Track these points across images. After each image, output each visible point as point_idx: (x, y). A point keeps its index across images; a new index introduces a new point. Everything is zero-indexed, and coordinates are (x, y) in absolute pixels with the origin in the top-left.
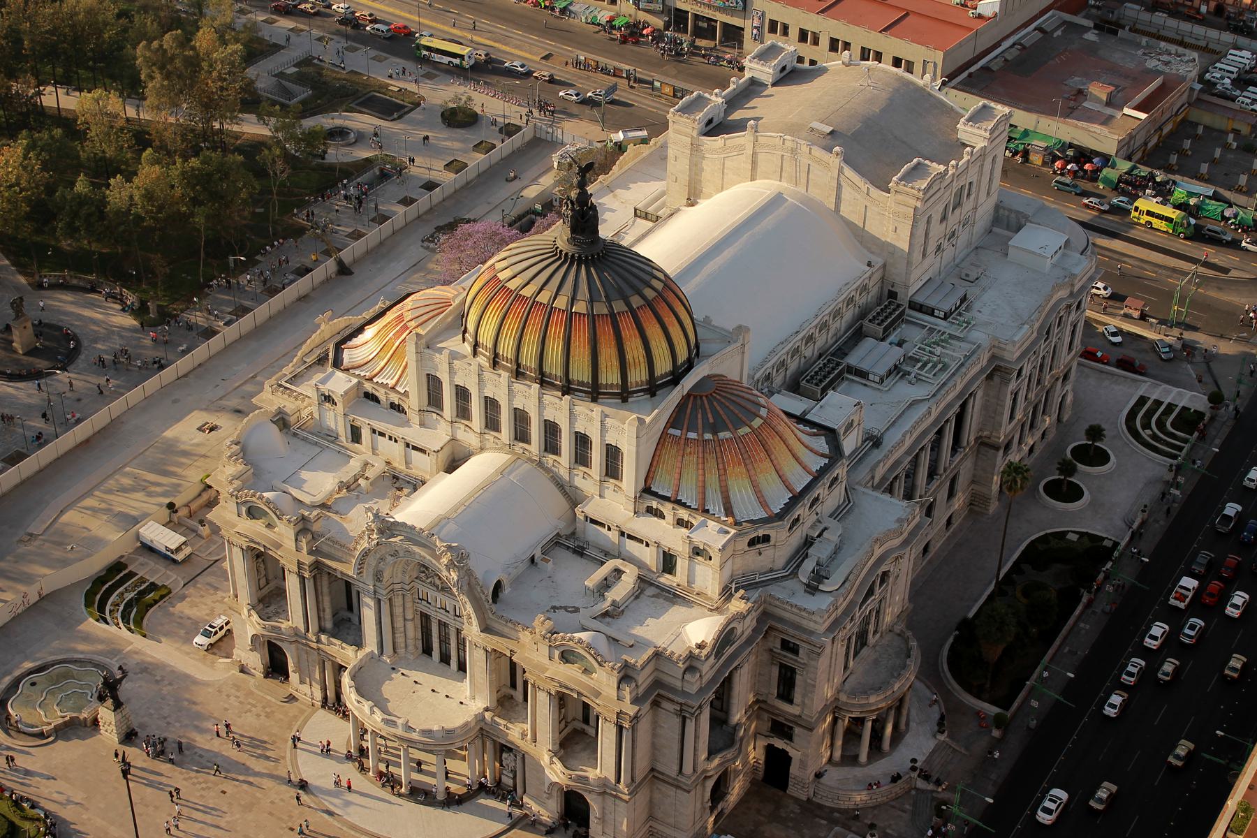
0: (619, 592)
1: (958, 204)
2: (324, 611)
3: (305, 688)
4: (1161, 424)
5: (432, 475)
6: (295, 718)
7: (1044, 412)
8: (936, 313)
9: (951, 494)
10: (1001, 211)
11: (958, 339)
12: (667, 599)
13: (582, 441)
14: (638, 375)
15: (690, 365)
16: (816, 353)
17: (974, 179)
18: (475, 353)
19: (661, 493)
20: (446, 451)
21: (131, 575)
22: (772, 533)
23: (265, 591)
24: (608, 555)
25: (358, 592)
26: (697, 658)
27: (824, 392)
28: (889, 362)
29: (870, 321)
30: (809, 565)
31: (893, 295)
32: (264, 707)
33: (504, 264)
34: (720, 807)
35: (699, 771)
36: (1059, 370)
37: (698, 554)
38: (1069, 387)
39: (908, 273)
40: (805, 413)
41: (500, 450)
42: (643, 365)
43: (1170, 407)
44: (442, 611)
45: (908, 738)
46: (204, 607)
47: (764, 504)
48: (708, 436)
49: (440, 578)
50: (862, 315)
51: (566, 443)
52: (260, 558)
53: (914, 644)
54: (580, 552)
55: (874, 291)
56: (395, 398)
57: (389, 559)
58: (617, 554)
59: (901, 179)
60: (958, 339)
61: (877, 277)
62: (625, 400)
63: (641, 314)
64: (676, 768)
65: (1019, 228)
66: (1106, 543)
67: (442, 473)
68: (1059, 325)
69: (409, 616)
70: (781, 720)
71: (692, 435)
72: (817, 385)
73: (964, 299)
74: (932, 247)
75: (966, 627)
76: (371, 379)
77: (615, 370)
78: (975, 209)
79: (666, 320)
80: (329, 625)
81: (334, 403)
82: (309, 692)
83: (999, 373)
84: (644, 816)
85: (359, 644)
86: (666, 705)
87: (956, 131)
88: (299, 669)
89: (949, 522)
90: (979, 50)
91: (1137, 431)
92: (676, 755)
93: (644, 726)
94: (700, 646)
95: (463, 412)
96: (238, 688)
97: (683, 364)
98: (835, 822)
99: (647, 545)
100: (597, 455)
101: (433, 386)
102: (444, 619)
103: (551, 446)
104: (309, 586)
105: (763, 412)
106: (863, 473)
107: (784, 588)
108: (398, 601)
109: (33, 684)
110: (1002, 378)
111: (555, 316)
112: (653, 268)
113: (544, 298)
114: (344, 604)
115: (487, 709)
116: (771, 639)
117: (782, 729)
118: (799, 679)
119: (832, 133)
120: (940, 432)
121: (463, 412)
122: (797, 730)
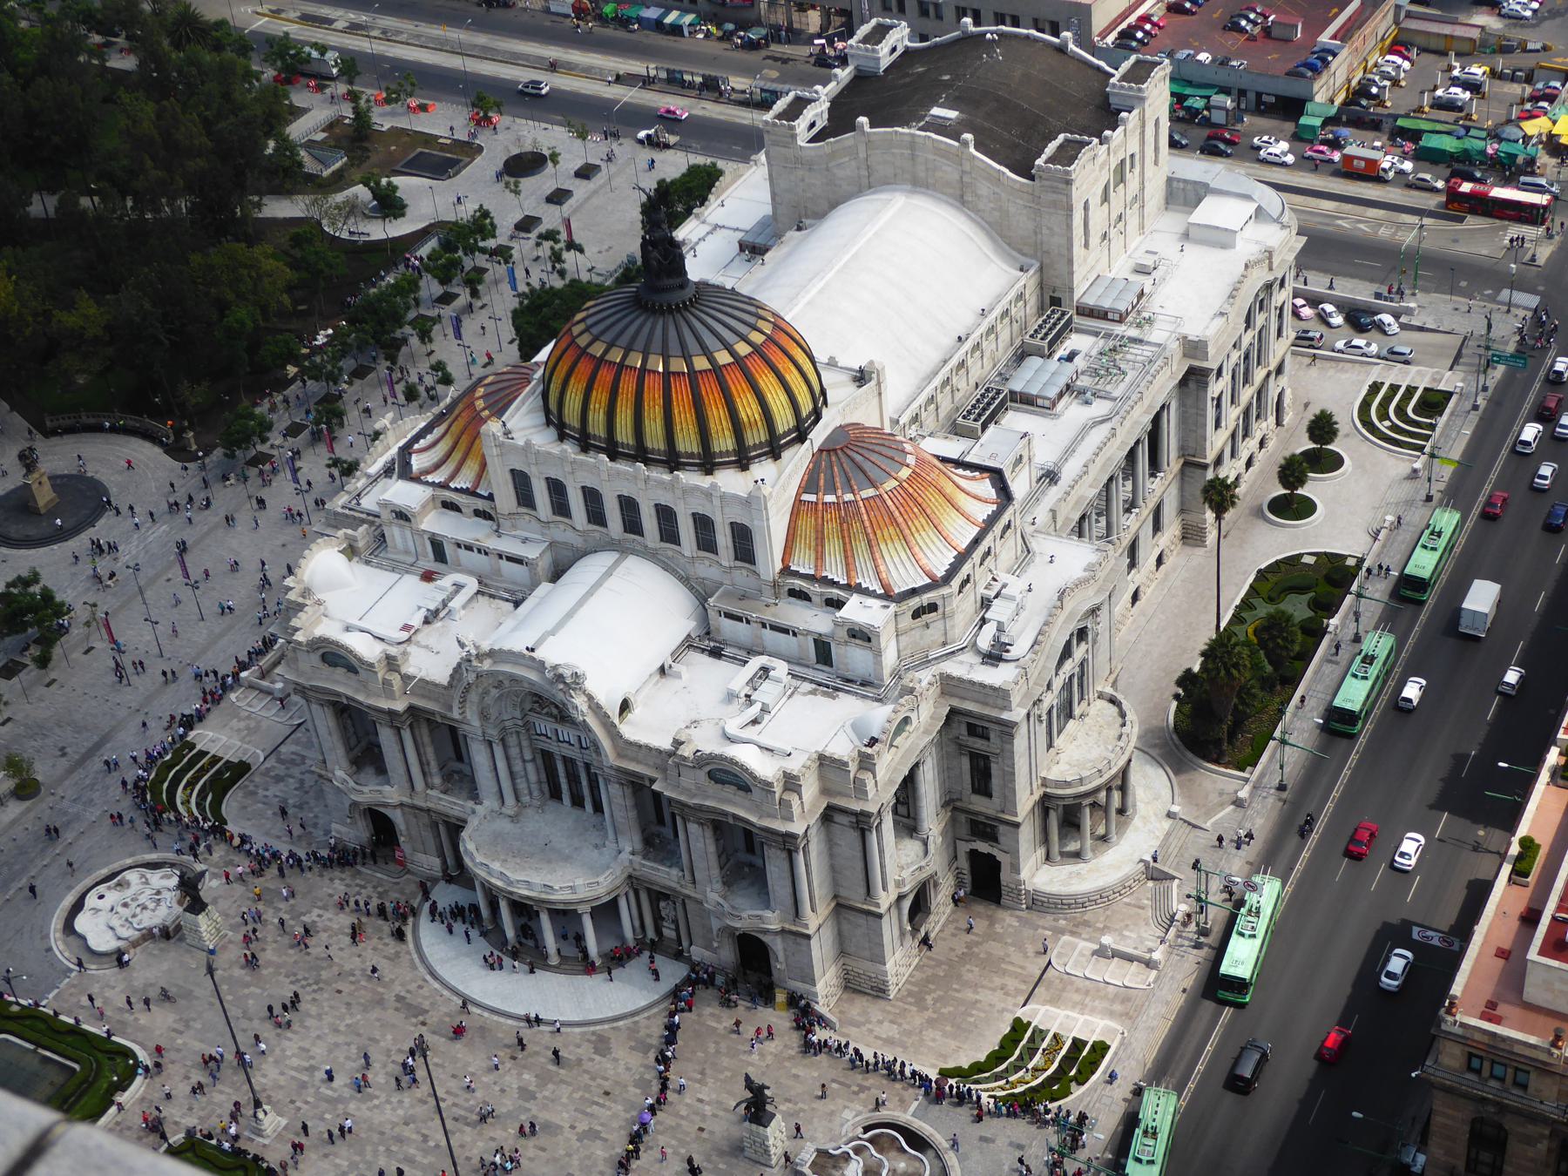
0: (767, 692)
2: (428, 764)
4: (1400, 410)
7: (1258, 417)
8: (1110, 316)
9: (1157, 527)
10: (1175, 184)
11: (1141, 341)
12: (825, 694)
13: (703, 524)
16: (972, 382)
18: (562, 437)
19: (802, 571)
21: (203, 754)
22: (939, 603)
23: (357, 751)
24: (752, 652)
25: (465, 737)
26: (870, 757)
27: (984, 427)
28: (1062, 382)
29: (1032, 336)
30: (989, 630)
31: (1056, 302)
32: (375, 887)
33: (582, 327)
35: (891, 886)
37: (854, 636)
38: (1283, 381)
42: (759, 424)
43: (1410, 391)
44: (565, 745)
45: (1137, 821)
46: (291, 780)
48: (849, 497)
49: (557, 707)
54: (716, 653)
56: (481, 504)
57: (494, 692)
58: (761, 650)
59: (1046, 162)
60: (1141, 341)
64: (862, 891)
65: (1200, 201)
66: (1351, 562)
67: (545, 587)
68: (1261, 309)
69: (528, 756)
70: (982, 819)
71: (830, 498)
72: (975, 420)
73: (1141, 295)
75: (1187, 679)
76: (444, 486)
77: (727, 433)
78: (1142, 183)
80: (437, 780)
81: (407, 519)
82: (429, 863)
83: (1193, 377)
85: (474, 796)
87: (1107, 96)
89: (1159, 561)
91: (1373, 424)
92: (861, 876)
93: (816, 847)
95: (561, 507)
97: (808, 417)
98: (1062, 932)
99: (795, 634)
100: (724, 539)
101: (521, 482)
103: (669, 533)
104: (407, 735)
105: (910, 460)
106: (1041, 513)
107: (961, 663)
108: (512, 740)
109: (101, 897)
110: (1198, 382)
111: (649, 381)
112: (758, 307)
114: (452, 754)
115: (633, 853)
116: (954, 725)
118: (995, 769)
120: (1131, 455)
121: (561, 507)
122: (1002, 828)
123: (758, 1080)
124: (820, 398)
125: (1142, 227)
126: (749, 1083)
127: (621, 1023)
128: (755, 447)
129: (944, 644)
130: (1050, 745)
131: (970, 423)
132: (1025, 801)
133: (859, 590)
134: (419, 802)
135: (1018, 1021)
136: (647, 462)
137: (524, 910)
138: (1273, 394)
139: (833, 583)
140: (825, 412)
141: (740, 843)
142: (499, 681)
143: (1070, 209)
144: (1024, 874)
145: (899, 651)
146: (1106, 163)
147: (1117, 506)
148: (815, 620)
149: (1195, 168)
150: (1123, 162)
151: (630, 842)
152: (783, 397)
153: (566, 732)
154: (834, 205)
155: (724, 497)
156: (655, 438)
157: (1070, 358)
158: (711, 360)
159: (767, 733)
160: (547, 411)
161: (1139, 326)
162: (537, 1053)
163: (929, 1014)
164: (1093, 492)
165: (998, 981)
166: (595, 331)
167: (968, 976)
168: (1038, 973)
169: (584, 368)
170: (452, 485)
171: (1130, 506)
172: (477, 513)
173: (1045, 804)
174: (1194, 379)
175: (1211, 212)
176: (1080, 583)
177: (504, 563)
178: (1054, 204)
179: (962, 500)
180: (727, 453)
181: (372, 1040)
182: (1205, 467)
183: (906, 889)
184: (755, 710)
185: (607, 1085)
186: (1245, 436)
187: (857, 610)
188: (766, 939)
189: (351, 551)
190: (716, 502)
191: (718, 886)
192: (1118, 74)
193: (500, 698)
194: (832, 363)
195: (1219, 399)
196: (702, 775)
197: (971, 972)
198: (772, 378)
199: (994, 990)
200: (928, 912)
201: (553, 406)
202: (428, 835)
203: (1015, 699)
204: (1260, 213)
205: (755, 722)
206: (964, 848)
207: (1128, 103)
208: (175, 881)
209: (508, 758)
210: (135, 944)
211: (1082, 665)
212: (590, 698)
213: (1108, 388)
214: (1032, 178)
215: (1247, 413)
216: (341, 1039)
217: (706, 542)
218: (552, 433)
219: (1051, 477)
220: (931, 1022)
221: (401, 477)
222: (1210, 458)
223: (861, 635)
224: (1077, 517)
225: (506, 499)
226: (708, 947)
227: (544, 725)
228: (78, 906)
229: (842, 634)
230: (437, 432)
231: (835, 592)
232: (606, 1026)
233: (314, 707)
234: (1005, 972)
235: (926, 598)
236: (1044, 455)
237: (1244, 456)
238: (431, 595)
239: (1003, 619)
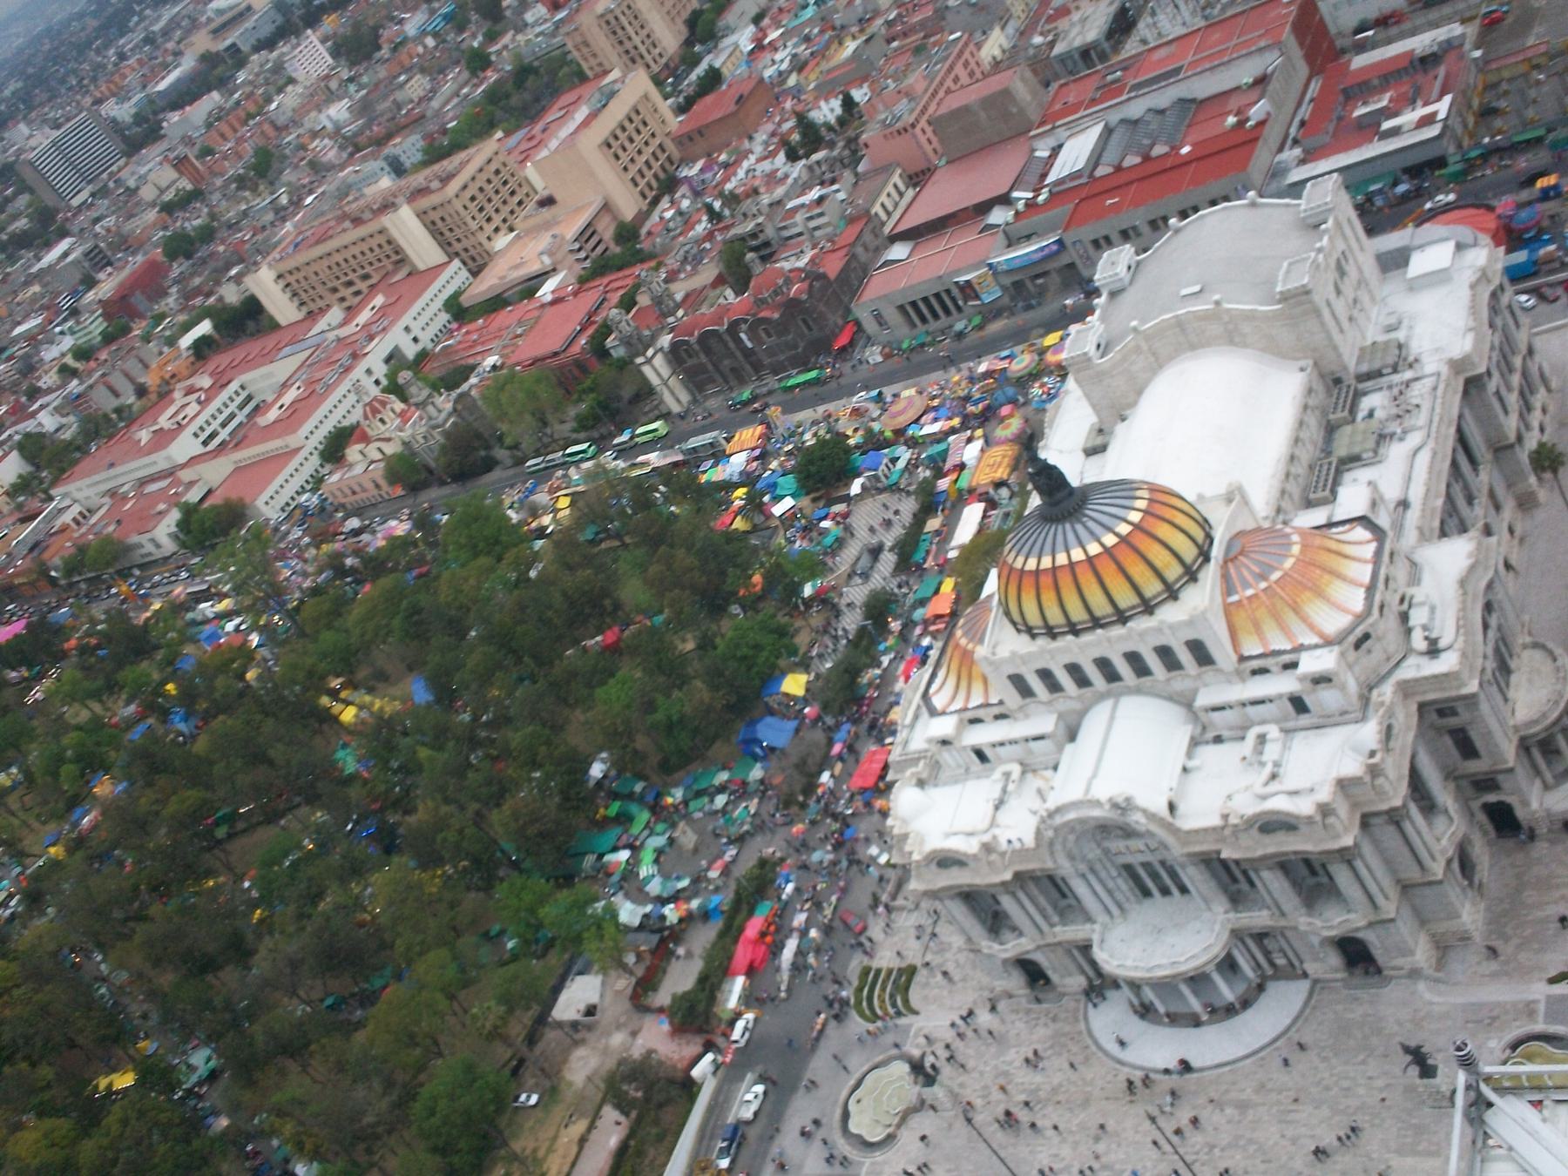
0: (1271, 751)
5: (1060, 749)
6: (1076, 1010)
9: (1498, 507)
11: (1416, 379)
13: (1165, 653)
14: (1173, 571)
15: (1210, 538)
18: (1033, 636)
21: (878, 972)
22: (1370, 630)
23: (989, 922)
25: (1063, 879)
27: (1334, 493)
31: (1338, 381)
34: (1476, 881)
35: (1438, 856)
36: (1523, 348)
38: (1537, 358)
39: (1339, 356)
40: (1329, 517)
41: (1102, 697)
47: (1346, 611)
48: (1263, 585)
50: (1324, 413)
51: (1153, 662)
52: (969, 897)
54: (1218, 740)
55: (1319, 388)
56: (996, 711)
60: (1416, 379)
61: (1315, 374)
63: (1145, 525)
64: (1416, 868)
67: (1069, 747)
69: (1114, 873)
76: (965, 709)
79: (1167, 516)
80: (1056, 919)
85: (1089, 919)
86: (1375, 821)
88: (1055, 970)
93: (1367, 849)
95: (1054, 686)
100: (1184, 656)
101: (1018, 682)
102: (1148, 858)
103: (1141, 669)
106: (1410, 536)
108: (1098, 867)
114: (1056, 895)
117: (1487, 783)
118: (1474, 735)
119: (1201, 291)
120: (1454, 464)
121: (1054, 686)
122: (1500, 778)
123: (1413, 1044)
124: (1205, 524)
125: (1373, 299)
126: (1407, 1050)
127: (1279, 1043)
128: (1177, 580)
129: (1388, 659)
130: (1506, 700)
131: (1320, 494)
132: (1509, 751)
133: (1300, 648)
134: (1050, 940)
136: (1102, 626)
137: (1165, 986)
138: (1534, 371)
140: (1213, 533)
141: (1304, 871)
142: (1070, 827)
143: (1317, 313)
144: (1535, 805)
145: (1357, 679)
146: (1327, 266)
147: (1461, 502)
148: (1280, 685)
149: (1391, 241)
150: (1338, 261)
151: (1220, 906)
152: (1181, 537)
153: (1137, 844)
154: (1140, 392)
155: (1172, 627)
156: (1101, 606)
157: (1371, 415)
158: (1117, 535)
159: (1290, 781)
160: (1014, 623)
161: (1411, 366)
162: (1227, 1091)
163: (1515, 941)
164: (1440, 502)
165: (1557, 894)
166: (1026, 549)
169: (1028, 583)
170: (971, 705)
171: (1470, 500)
172: (998, 717)
173: (1524, 746)
174: (1473, 386)
175: (1420, 264)
176: (1472, 568)
177: (1033, 745)
179: (1349, 550)
180: (1159, 594)
182: (1511, 446)
183: (1450, 853)
184: (1268, 769)
185: (1292, 1094)
187: (1312, 663)
188: (1360, 935)
189: (921, 783)
190: (1167, 631)
191: (1303, 910)
193: (1078, 839)
194: (1201, 497)
195: (1498, 393)
196: (1254, 832)
197: (1530, 896)
198: (1166, 526)
199: (1556, 902)
200: (1473, 867)
202: (1067, 962)
203: (1465, 675)
204: (1460, 247)
205: (1274, 776)
206: (1476, 805)
207: (1321, 217)
208: (906, 1068)
209: (1101, 881)
210: (899, 1126)
212: (1144, 811)
213: (1413, 422)
215: (1522, 393)
218: (1025, 638)
219: (1404, 504)
220: (1519, 947)
222: (1512, 437)
223: (1321, 680)
224: (1437, 524)
225: (1013, 699)
226: (1316, 959)
227: (1117, 845)
228: (846, 1115)
229: (1308, 685)
230: (941, 674)
231: (1287, 658)
234: (1558, 886)
235: (1359, 632)
236: (1392, 493)
237: (1535, 424)
239: (1424, 621)
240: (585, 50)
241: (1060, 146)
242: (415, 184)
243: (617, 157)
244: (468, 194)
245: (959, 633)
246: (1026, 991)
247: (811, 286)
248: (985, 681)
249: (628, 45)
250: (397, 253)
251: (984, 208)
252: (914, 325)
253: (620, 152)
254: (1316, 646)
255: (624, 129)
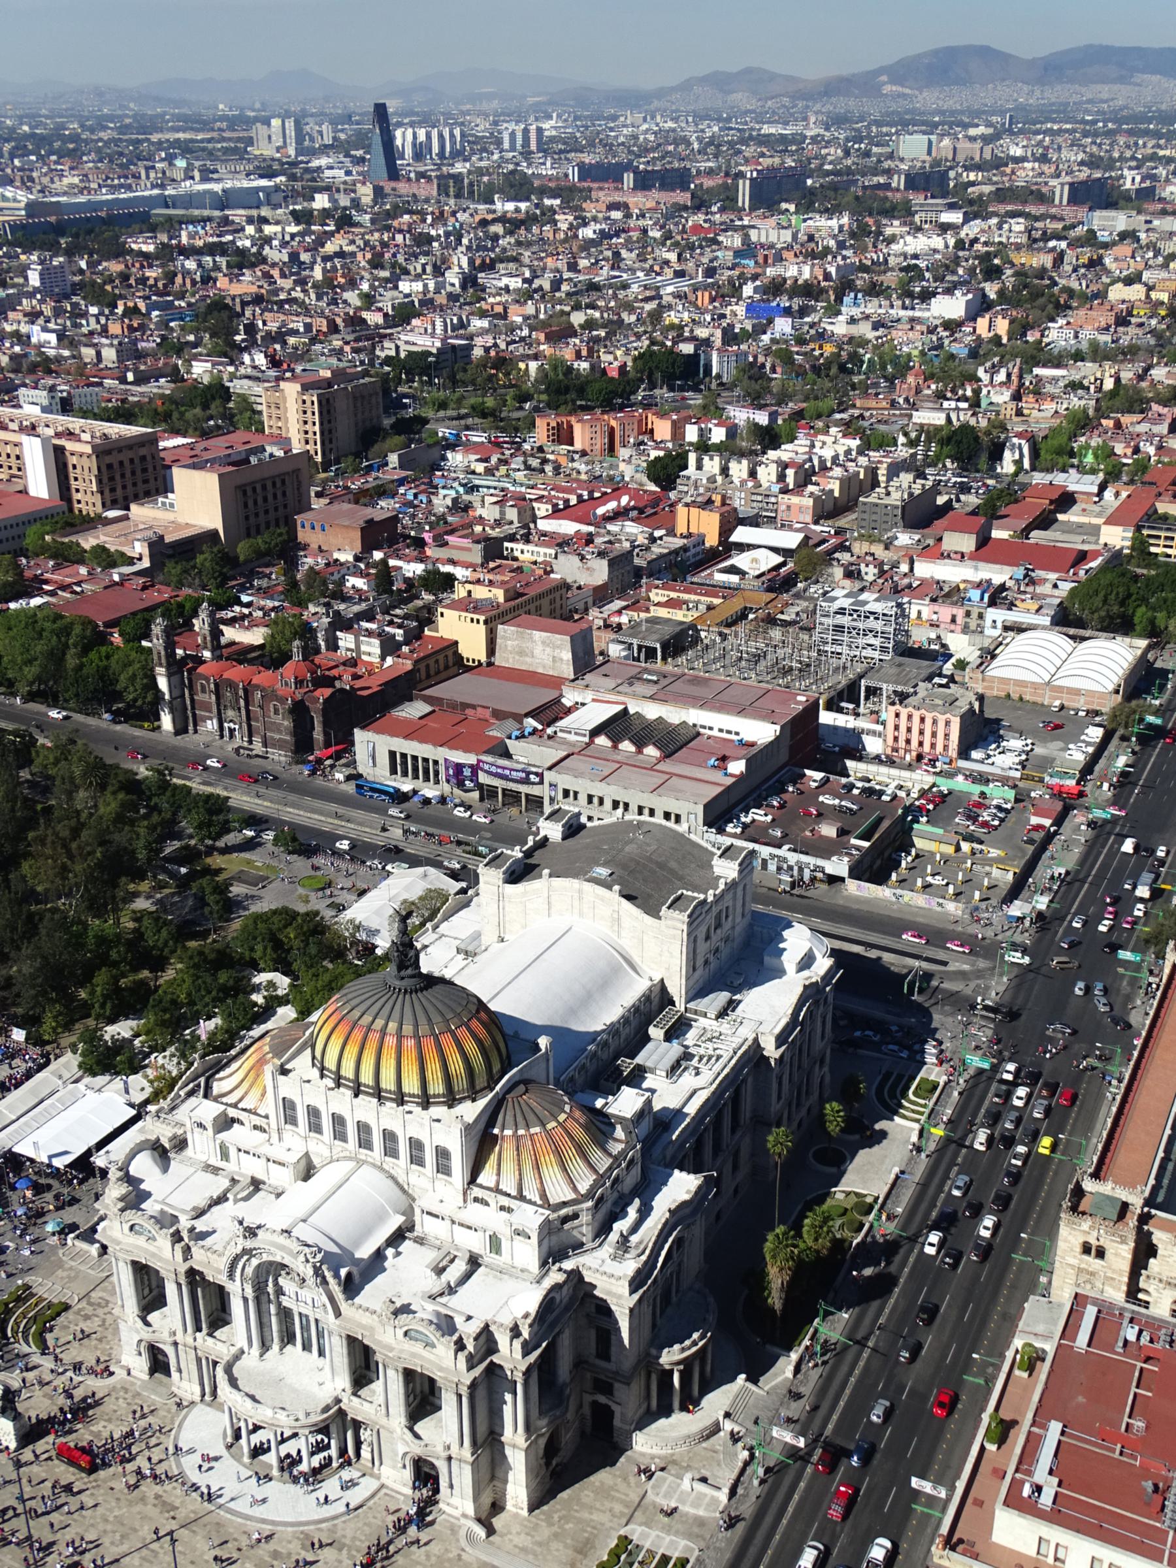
1: (718, 926)
3: (185, 1384)
7: (807, 1093)
9: (735, 1167)
14: (461, 1083)
17: (730, 904)
18: (322, 1076)
20: (303, 1163)
21: (33, 1295)
30: (614, 1237)
34: (554, 1463)
41: (350, 1159)
47: (575, 1189)
53: (711, 1300)
54: (420, 1241)
61: (658, 988)
62: (450, 1107)
66: (869, 1200)
67: (300, 1183)
70: (603, 1377)
74: (700, 962)
76: (235, 1106)
78: (733, 928)
81: (205, 1128)
84: (488, 1477)
88: (180, 1371)
89: (736, 1191)
90: (732, 801)
94: (526, 1316)
95: (316, 1128)
96: (126, 1390)
100: (429, 1157)
101: (288, 1106)
102: (304, 1311)
103: (391, 1150)
108: (264, 1298)
113: (379, 1023)
121: (316, 1128)
122: (617, 1385)
127: (324, 1525)
135: (620, 1537)
136: (380, 1098)
139: (509, 1195)
151: (342, 1382)
153: (306, 1294)
156: (388, 1082)
160: (314, 1058)
165: (608, 1505)
167: (585, 1500)
168: (637, 1500)
172: (255, 1127)
178: (674, 937)
180: (438, 1096)
181: (135, 1530)
186: (798, 1105)
192: (719, 853)
196: (400, 1333)
201: (318, 1054)
206: (588, 1398)
211: (680, 1265)
214: (659, 918)
216: (109, 1527)
217: (417, 1158)
218: (315, 1073)
220: (556, 1536)
221: (206, 1096)
226: (394, 1467)
230: (235, 1066)
232: (312, 1527)
233: (121, 1264)
238: (220, 1184)
240: (274, 411)
241: (583, 704)
242: (70, 426)
243: (246, 505)
244: (108, 459)
245: (267, 1039)
246: (145, 1377)
247: (333, 694)
248: (263, 1094)
249: (308, 427)
250: (19, 469)
251: (499, 715)
252: (393, 771)
253: (251, 503)
254: (534, 1204)
255: (264, 488)
